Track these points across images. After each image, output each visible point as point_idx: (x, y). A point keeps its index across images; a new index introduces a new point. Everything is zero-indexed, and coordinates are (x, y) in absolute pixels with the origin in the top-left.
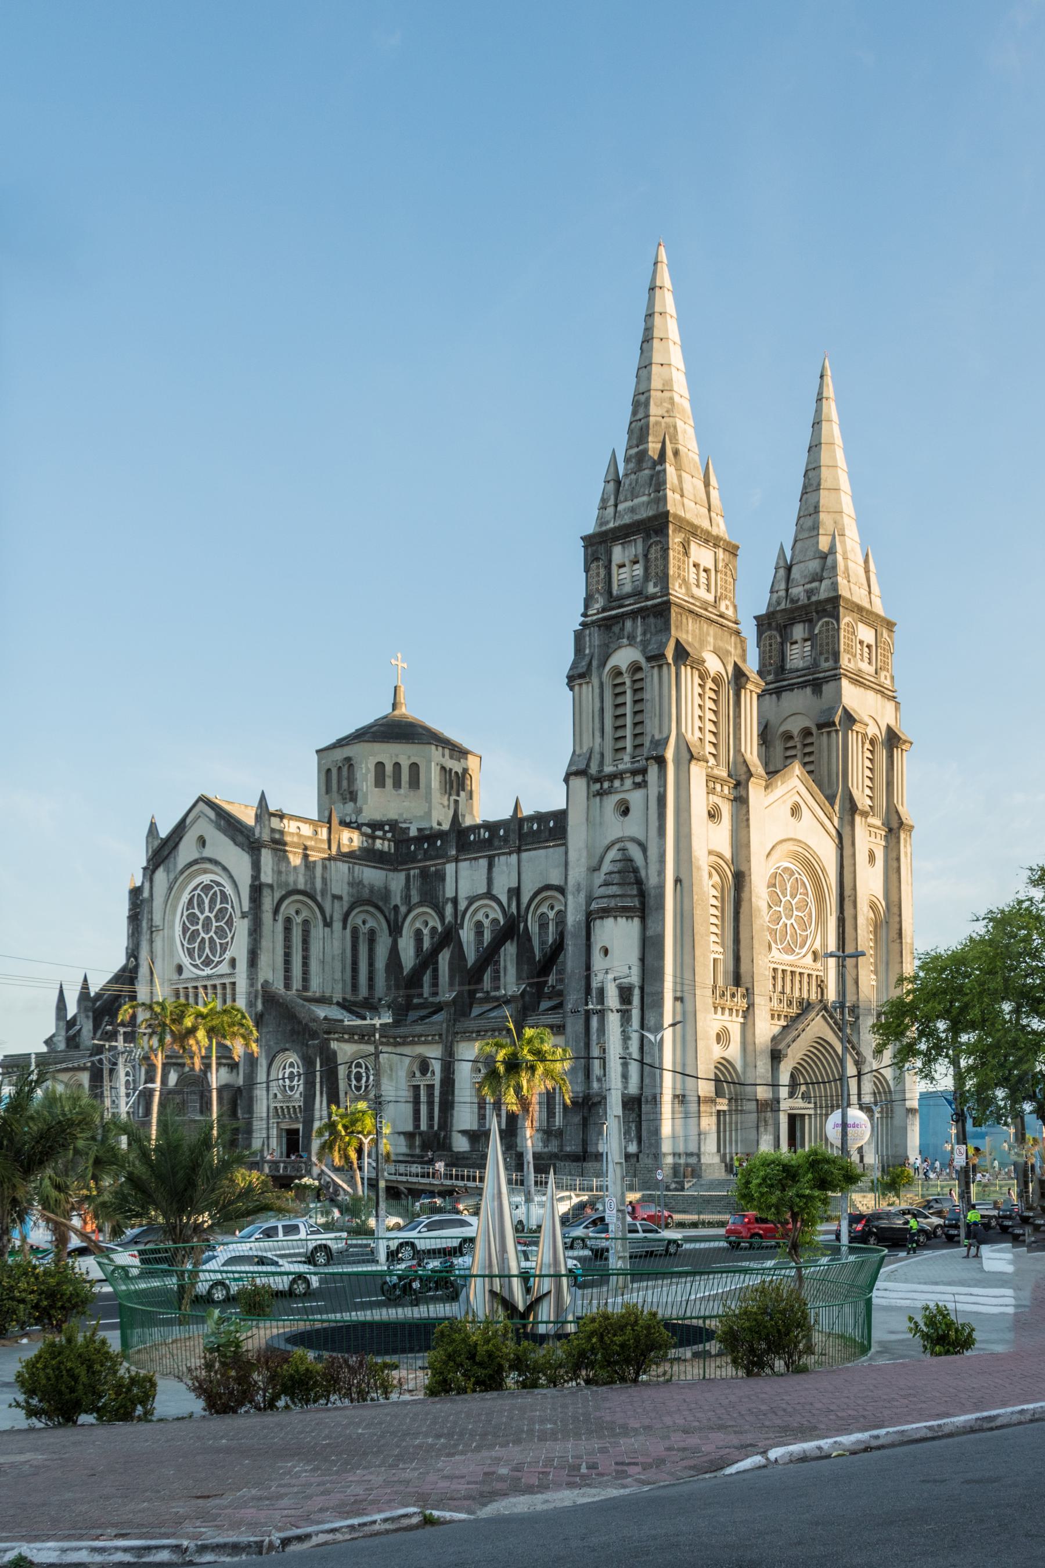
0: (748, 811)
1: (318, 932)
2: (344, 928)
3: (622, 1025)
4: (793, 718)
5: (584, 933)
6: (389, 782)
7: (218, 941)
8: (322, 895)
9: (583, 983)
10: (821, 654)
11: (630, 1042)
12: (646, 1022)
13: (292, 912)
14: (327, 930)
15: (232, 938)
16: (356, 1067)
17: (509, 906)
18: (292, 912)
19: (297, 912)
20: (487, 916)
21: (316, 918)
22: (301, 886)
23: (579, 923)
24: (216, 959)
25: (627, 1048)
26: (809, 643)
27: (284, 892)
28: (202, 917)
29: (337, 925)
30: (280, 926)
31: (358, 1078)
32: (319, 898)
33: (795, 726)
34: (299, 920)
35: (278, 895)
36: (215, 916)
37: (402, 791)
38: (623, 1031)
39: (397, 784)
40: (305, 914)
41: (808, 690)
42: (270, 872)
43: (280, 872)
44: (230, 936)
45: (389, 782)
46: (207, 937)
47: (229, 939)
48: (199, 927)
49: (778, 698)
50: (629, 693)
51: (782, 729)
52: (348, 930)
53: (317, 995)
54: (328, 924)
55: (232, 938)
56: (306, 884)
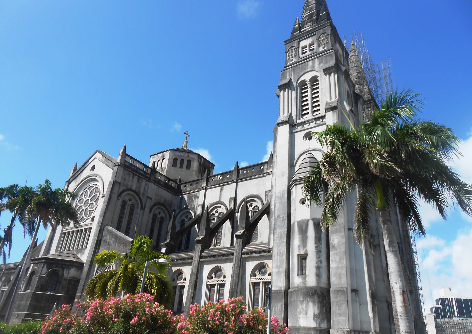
1: (138, 211)
2: (150, 212)
5: (286, 196)
6: (178, 165)
7: (89, 209)
8: (143, 195)
9: (286, 222)
12: (331, 242)
13: (127, 198)
15: (96, 208)
17: (230, 205)
18: (127, 198)
19: (130, 200)
20: (217, 212)
21: (138, 205)
22: (134, 188)
23: (284, 191)
24: (86, 218)
27: (125, 188)
28: (85, 200)
29: (147, 210)
30: (119, 203)
32: (141, 196)
34: (130, 203)
35: (121, 189)
36: (91, 200)
37: (183, 169)
39: (181, 167)
40: (133, 201)
43: (125, 179)
44: (95, 207)
45: (178, 165)
46: (85, 208)
47: (94, 208)
48: (83, 204)
50: (309, 90)
52: (152, 214)
54: (143, 208)
55: (96, 208)
56: (136, 188)
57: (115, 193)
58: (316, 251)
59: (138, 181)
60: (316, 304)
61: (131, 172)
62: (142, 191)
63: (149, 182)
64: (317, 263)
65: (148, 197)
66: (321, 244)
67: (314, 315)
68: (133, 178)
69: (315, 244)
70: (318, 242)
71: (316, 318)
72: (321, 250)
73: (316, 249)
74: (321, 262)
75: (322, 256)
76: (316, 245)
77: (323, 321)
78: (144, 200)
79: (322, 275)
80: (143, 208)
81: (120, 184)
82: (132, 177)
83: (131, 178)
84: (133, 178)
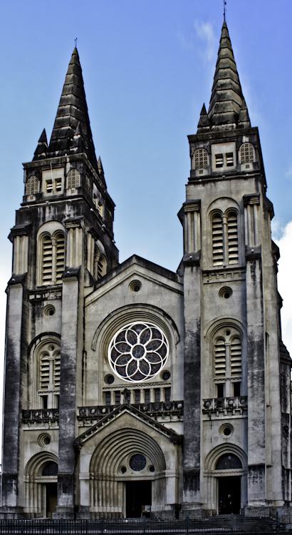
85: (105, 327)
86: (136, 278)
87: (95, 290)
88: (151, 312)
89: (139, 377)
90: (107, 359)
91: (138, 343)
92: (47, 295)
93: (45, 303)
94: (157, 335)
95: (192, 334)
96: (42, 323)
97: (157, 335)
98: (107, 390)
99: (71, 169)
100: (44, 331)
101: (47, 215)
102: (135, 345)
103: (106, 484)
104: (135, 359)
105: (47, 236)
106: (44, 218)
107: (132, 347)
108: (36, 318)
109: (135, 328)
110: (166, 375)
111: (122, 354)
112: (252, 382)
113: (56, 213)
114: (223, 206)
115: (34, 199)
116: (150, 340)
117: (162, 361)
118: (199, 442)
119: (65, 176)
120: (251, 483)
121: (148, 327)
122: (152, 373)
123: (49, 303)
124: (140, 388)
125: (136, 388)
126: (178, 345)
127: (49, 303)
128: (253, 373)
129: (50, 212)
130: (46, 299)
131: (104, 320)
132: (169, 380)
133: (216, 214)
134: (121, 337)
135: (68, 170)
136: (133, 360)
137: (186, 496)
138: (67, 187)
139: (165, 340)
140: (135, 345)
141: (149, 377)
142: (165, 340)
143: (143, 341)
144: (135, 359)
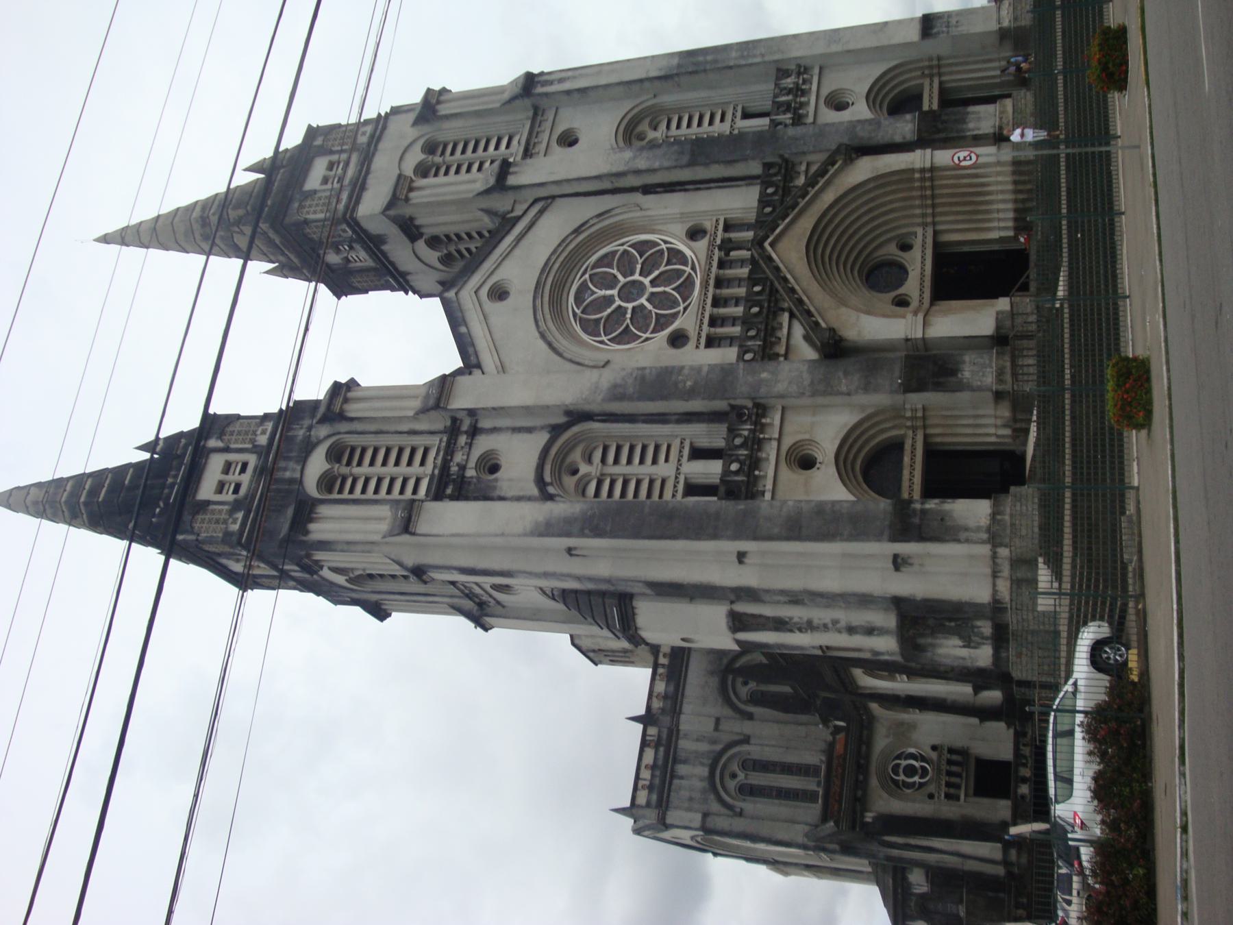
0: (483, 409)
1: (755, 751)
2: (750, 716)
3: (791, 631)
4: (423, 258)
10: (340, 236)
11: (816, 622)
13: (732, 785)
14: (752, 741)
16: (897, 774)
19: (734, 776)
21: (739, 753)
22: (704, 771)
25: (825, 626)
26: (341, 247)
27: (712, 796)
29: (747, 727)
30: (749, 806)
31: (910, 771)
32: (718, 747)
33: (432, 256)
34: (741, 776)
35: (715, 807)
38: (800, 630)
40: (735, 767)
41: (385, 248)
42: (690, 815)
43: (691, 799)
49: (409, 274)
51: (441, 267)
53: (824, 758)
54: (746, 740)
56: (702, 764)
57: (731, 825)
58: (812, 632)
59: (685, 762)
60: (938, 641)
61: (670, 784)
62: (704, 747)
63: (678, 731)
64: (840, 632)
65: (716, 729)
66: (791, 619)
67: (964, 646)
68: (682, 778)
69: (794, 632)
70: (788, 626)
71: (972, 644)
72: (805, 619)
73: (806, 631)
74: (835, 622)
75: (820, 619)
76: (797, 631)
77: (976, 630)
78: (726, 738)
79: (868, 622)
80: (746, 740)
81: (705, 815)
82: (683, 781)
83: (683, 782)
84: (682, 778)
85: (564, 342)
86: (484, 292)
87: (479, 366)
88: (561, 259)
89: (686, 288)
90: (630, 349)
91: (614, 292)
92: (454, 469)
93: (471, 473)
94: (606, 261)
95: (635, 158)
96: (510, 480)
97: (606, 261)
98: (703, 341)
99: (220, 438)
100: (531, 474)
101: (288, 474)
102: (617, 298)
103: (944, 205)
104: (646, 296)
105: (328, 482)
106: (291, 481)
107: (618, 302)
108: (497, 493)
109: (579, 299)
110: (695, 234)
111: (628, 321)
112: (755, 56)
113: (294, 454)
114: (416, 156)
115: (240, 515)
116: (615, 271)
117: (664, 246)
118: (859, 121)
119: (226, 450)
120: (959, 29)
121: (587, 276)
122: (685, 264)
123: (472, 464)
124: (713, 276)
125: (712, 282)
126: (645, 206)
127: (472, 464)
128: (736, 59)
129: (285, 469)
130: (463, 468)
131: (550, 345)
132: (708, 225)
133: (423, 170)
134: (591, 328)
135: (220, 444)
136: (648, 300)
137: (979, 129)
138: (249, 446)
139: (622, 245)
140: (617, 298)
141: (693, 268)
142: (622, 245)
143: (610, 282)
144: (646, 296)
